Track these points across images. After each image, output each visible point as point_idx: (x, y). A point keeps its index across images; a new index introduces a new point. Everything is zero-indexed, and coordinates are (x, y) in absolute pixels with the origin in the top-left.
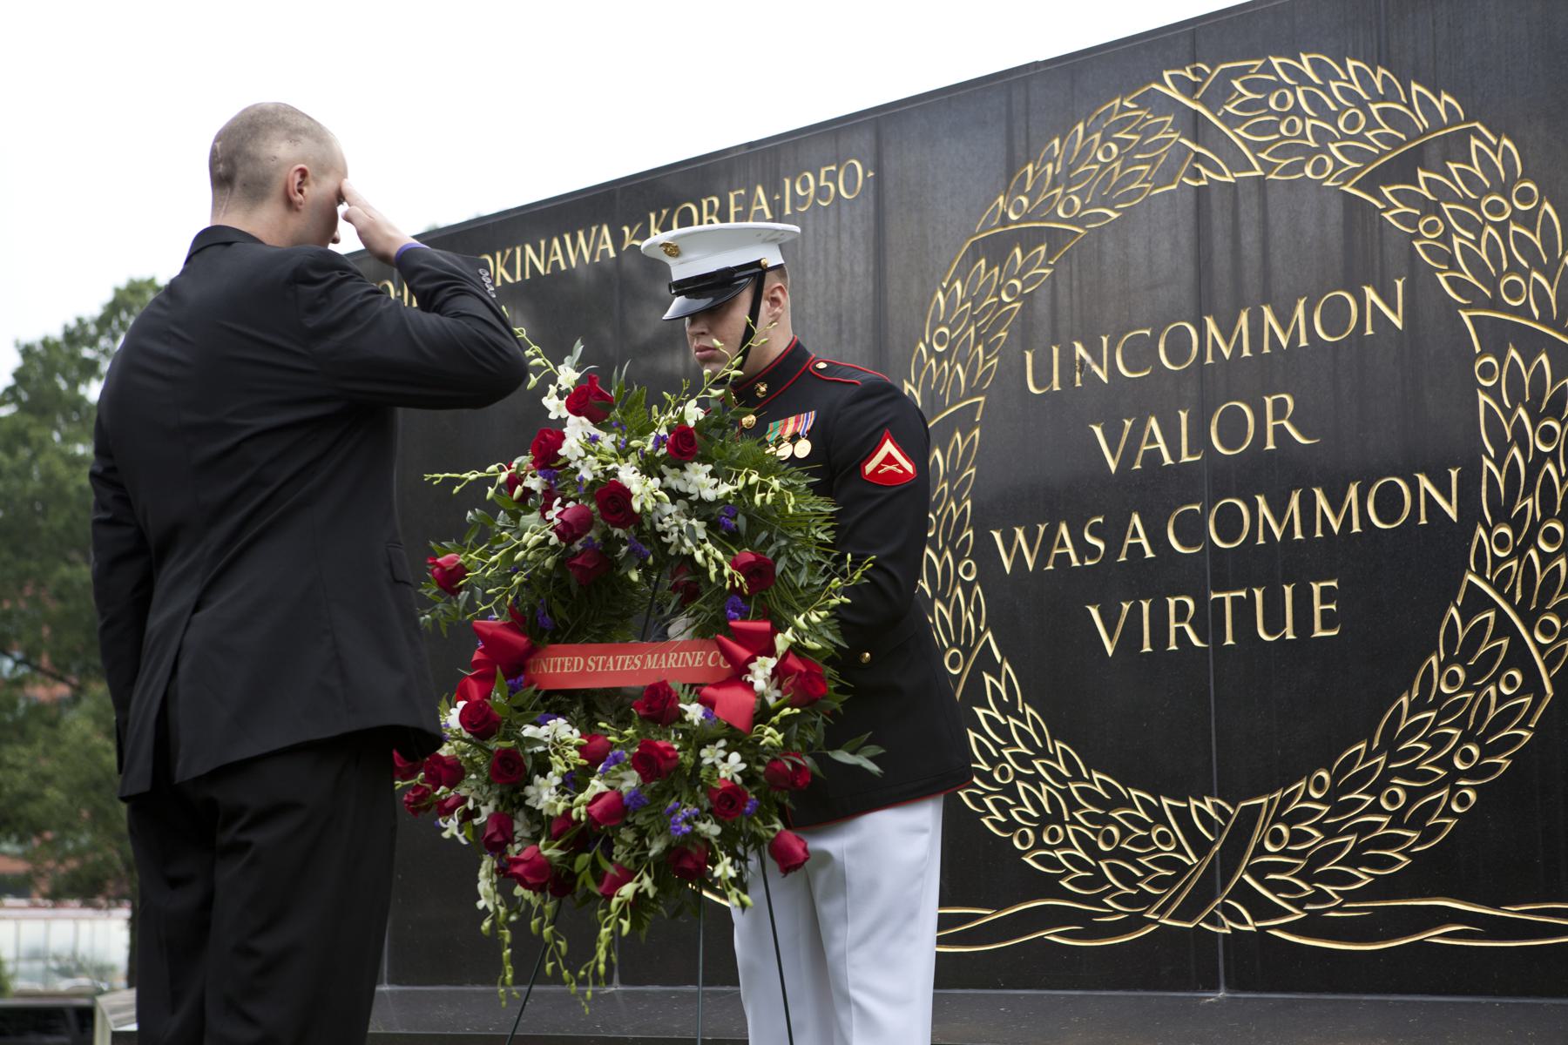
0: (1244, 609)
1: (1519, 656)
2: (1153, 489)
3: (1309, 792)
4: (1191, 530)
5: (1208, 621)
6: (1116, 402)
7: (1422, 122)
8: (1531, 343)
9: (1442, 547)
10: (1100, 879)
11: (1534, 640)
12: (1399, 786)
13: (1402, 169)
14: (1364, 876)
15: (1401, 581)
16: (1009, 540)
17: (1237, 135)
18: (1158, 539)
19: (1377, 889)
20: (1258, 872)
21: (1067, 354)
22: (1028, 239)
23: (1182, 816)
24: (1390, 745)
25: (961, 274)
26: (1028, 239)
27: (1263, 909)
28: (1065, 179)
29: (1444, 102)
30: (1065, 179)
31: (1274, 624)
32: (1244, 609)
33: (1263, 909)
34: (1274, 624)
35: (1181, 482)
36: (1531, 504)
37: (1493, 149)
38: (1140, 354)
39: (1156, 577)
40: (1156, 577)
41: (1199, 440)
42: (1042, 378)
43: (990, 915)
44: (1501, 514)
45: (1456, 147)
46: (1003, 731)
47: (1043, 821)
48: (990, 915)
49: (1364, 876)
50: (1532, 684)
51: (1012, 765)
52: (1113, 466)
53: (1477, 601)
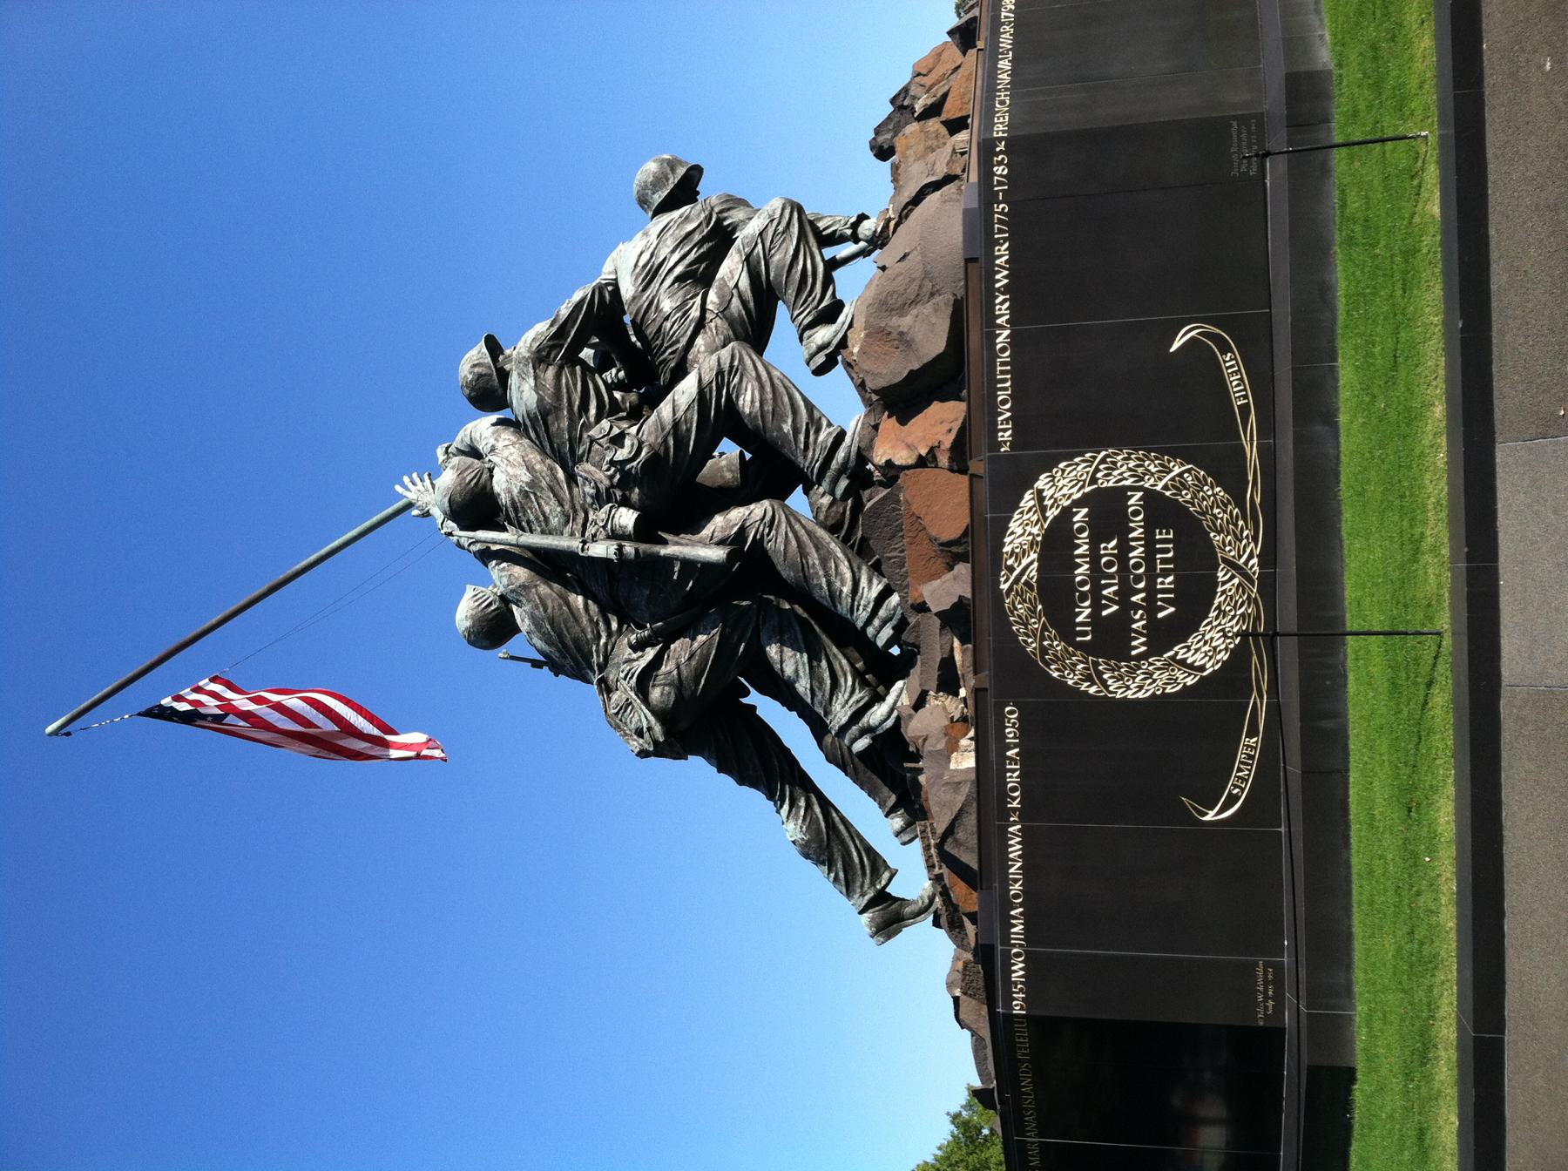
1: (1180, 475)
2: (1125, 592)
3: (1217, 539)
4: (1138, 579)
5: (1165, 573)
6: (1097, 607)
7: (1032, 503)
8: (1097, 470)
9: (1150, 497)
10: (1242, 615)
11: (1177, 470)
12: (1216, 511)
13: (1043, 509)
14: (1241, 523)
15: (1160, 509)
16: (1136, 648)
17: (1025, 562)
18: (1140, 591)
20: (1240, 557)
21: (1082, 624)
23: (1224, 583)
25: (1048, 665)
26: (1043, 638)
27: (1251, 556)
28: (1026, 625)
30: (1026, 625)
31: (1167, 550)
32: (1164, 561)
33: (1251, 556)
34: (1167, 550)
36: (1140, 470)
37: (1042, 482)
38: (1083, 597)
39: (1151, 591)
40: (1151, 591)
41: (1111, 577)
42: (1085, 634)
43: (1255, 657)
45: (1040, 492)
46: (1197, 650)
47: (1225, 636)
48: (1255, 657)
49: (1241, 523)
50: (1189, 471)
51: (1207, 648)
52: (1116, 607)
53: (1166, 487)
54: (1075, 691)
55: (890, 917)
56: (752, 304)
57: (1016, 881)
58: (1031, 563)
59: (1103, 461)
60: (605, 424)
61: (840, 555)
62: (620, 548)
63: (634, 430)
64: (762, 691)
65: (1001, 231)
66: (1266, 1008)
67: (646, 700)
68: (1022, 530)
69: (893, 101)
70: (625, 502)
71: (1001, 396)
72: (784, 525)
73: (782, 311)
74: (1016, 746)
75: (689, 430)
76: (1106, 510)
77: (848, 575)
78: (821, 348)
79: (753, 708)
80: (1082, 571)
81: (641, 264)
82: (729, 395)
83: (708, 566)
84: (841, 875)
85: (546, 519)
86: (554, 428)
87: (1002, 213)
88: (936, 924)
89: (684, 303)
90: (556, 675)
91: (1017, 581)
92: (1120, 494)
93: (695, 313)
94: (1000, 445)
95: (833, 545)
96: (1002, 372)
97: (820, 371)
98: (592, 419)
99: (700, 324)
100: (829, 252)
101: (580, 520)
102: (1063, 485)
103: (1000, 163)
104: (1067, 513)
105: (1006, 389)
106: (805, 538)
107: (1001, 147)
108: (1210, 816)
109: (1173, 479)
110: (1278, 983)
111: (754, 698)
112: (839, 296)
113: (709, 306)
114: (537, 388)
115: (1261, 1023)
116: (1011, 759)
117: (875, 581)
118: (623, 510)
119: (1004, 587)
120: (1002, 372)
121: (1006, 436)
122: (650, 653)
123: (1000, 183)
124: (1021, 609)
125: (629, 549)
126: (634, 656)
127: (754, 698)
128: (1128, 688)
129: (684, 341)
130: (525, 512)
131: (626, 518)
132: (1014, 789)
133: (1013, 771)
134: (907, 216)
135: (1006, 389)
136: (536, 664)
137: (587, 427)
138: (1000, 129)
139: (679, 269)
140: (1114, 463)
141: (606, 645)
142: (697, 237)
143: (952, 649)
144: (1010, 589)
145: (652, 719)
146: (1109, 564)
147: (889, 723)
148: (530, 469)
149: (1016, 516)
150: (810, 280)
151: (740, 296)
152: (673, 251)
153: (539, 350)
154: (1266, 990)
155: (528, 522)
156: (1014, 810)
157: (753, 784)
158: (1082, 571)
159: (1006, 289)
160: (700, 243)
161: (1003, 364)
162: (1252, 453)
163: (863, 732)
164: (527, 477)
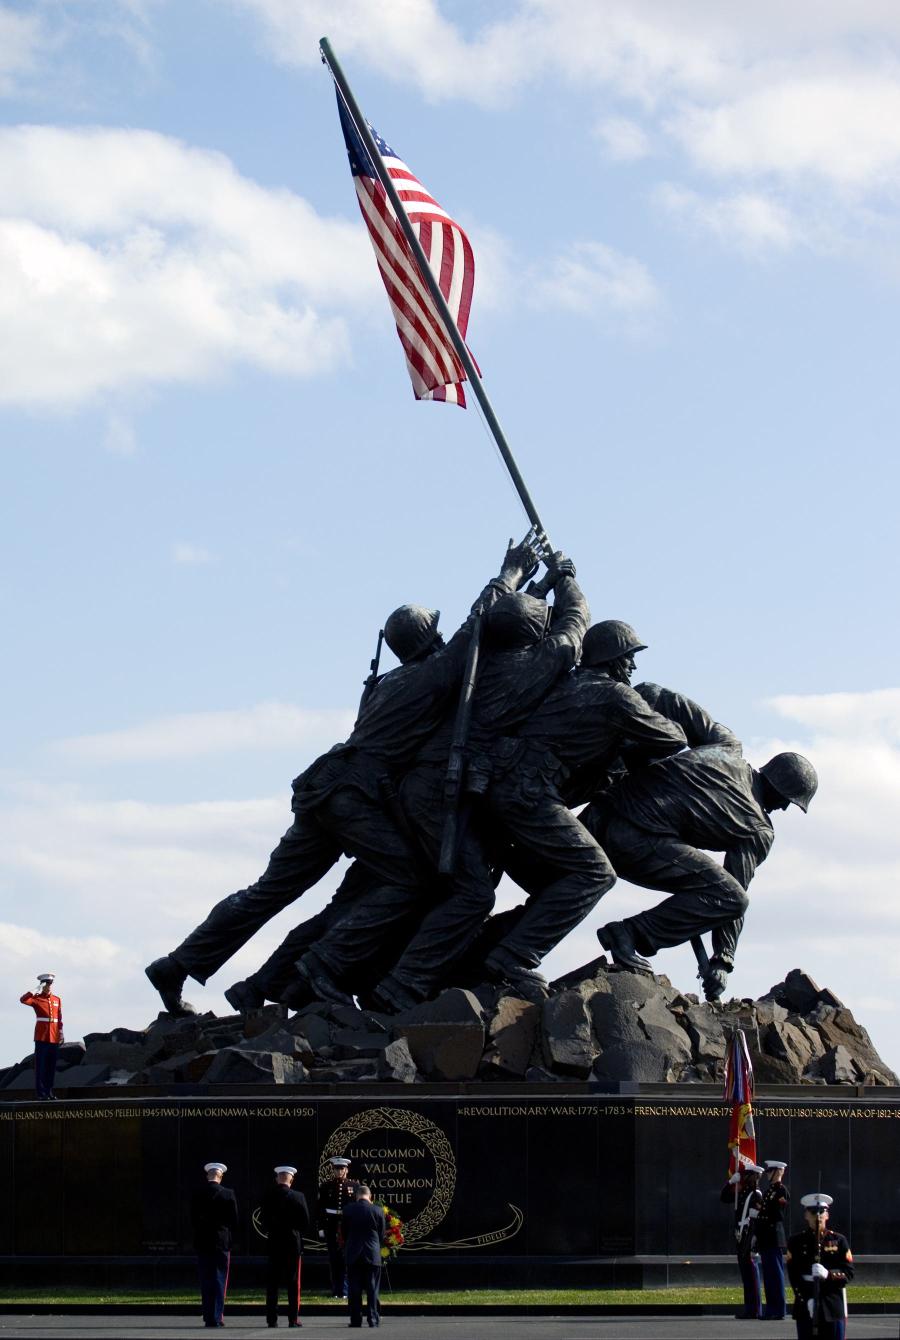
0: (394, 1198)
1: (441, 1208)
4: (384, 1183)
8: (445, 1162)
14: (414, 1239)
17: (395, 1121)
18: (377, 1184)
19: (416, 1241)
21: (360, 1153)
22: (352, 1131)
24: (419, 1220)
26: (352, 1131)
28: (360, 1121)
29: (432, 1123)
30: (360, 1121)
31: (400, 1199)
32: (394, 1198)
34: (400, 1199)
35: (382, 1176)
38: (374, 1153)
41: (386, 1169)
42: (354, 1154)
44: (439, 1187)
45: (434, 1131)
50: (443, 1212)
53: (434, 1199)
54: (322, 1148)
55: (166, 976)
57: (217, 1112)
58: (395, 1125)
59: (450, 1166)
61: (446, 958)
62: (455, 782)
63: (553, 791)
64: (350, 872)
66: (152, 1246)
68: (413, 1123)
69: (825, 991)
70: (492, 782)
71: (490, 1111)
74: (292, 1114)
76: (423, 1167)
77: (431, 965)
78: (616, 939)
79: (337, 860)
80: (389, 1153)
83: (437, 858)
84: (201, 942)
85: (486, 706)
87: (593, 1111)
88: (161, 1014)
90: (365, 683)
91: (385, 1116)
92: (431, 1175)
93: (656, 827)
94: (462, 1108)
95: (454, 952)
96: (503, 1110)
97: (601, 933)
98: (561, 754)
99: (646, 833)
100: (707, 939)
102: (439, 1143)
103: (620, 1110)
104: (421, 1145)
105: (493, 1112)
107: (629, 1111)
108: (255, 1219)
109: (439, 1203)
111: (344, 863)
112: (661, 951)
116: (284, 1111)
117: (423, 986)
119: (381, 1110)
120: (503, 1110)
121: (466, 1112)
123: (609, 1110)
124: (368, 1120)
125: (451, 790)
127: (344, 863)
128: (324, 1177)
131: (479, 786)
132: (267, 1112)
133: (278, 1112)
134: (681, 1024)
135: (493, 1112)
136: (375, 664)
138: (640, 1110)
140: (449, 1172)
143: (363, 1057)
144: (380, 1113)
146: (393, 1168)
147: (318, 992)
148: (528, 692)
149: (421, 1117)
154: (162, 1246)
156: (256, 1112)
158: (389, 1153)
161: (507, 1110)
162: (450, 1246)
163: (311, 971)
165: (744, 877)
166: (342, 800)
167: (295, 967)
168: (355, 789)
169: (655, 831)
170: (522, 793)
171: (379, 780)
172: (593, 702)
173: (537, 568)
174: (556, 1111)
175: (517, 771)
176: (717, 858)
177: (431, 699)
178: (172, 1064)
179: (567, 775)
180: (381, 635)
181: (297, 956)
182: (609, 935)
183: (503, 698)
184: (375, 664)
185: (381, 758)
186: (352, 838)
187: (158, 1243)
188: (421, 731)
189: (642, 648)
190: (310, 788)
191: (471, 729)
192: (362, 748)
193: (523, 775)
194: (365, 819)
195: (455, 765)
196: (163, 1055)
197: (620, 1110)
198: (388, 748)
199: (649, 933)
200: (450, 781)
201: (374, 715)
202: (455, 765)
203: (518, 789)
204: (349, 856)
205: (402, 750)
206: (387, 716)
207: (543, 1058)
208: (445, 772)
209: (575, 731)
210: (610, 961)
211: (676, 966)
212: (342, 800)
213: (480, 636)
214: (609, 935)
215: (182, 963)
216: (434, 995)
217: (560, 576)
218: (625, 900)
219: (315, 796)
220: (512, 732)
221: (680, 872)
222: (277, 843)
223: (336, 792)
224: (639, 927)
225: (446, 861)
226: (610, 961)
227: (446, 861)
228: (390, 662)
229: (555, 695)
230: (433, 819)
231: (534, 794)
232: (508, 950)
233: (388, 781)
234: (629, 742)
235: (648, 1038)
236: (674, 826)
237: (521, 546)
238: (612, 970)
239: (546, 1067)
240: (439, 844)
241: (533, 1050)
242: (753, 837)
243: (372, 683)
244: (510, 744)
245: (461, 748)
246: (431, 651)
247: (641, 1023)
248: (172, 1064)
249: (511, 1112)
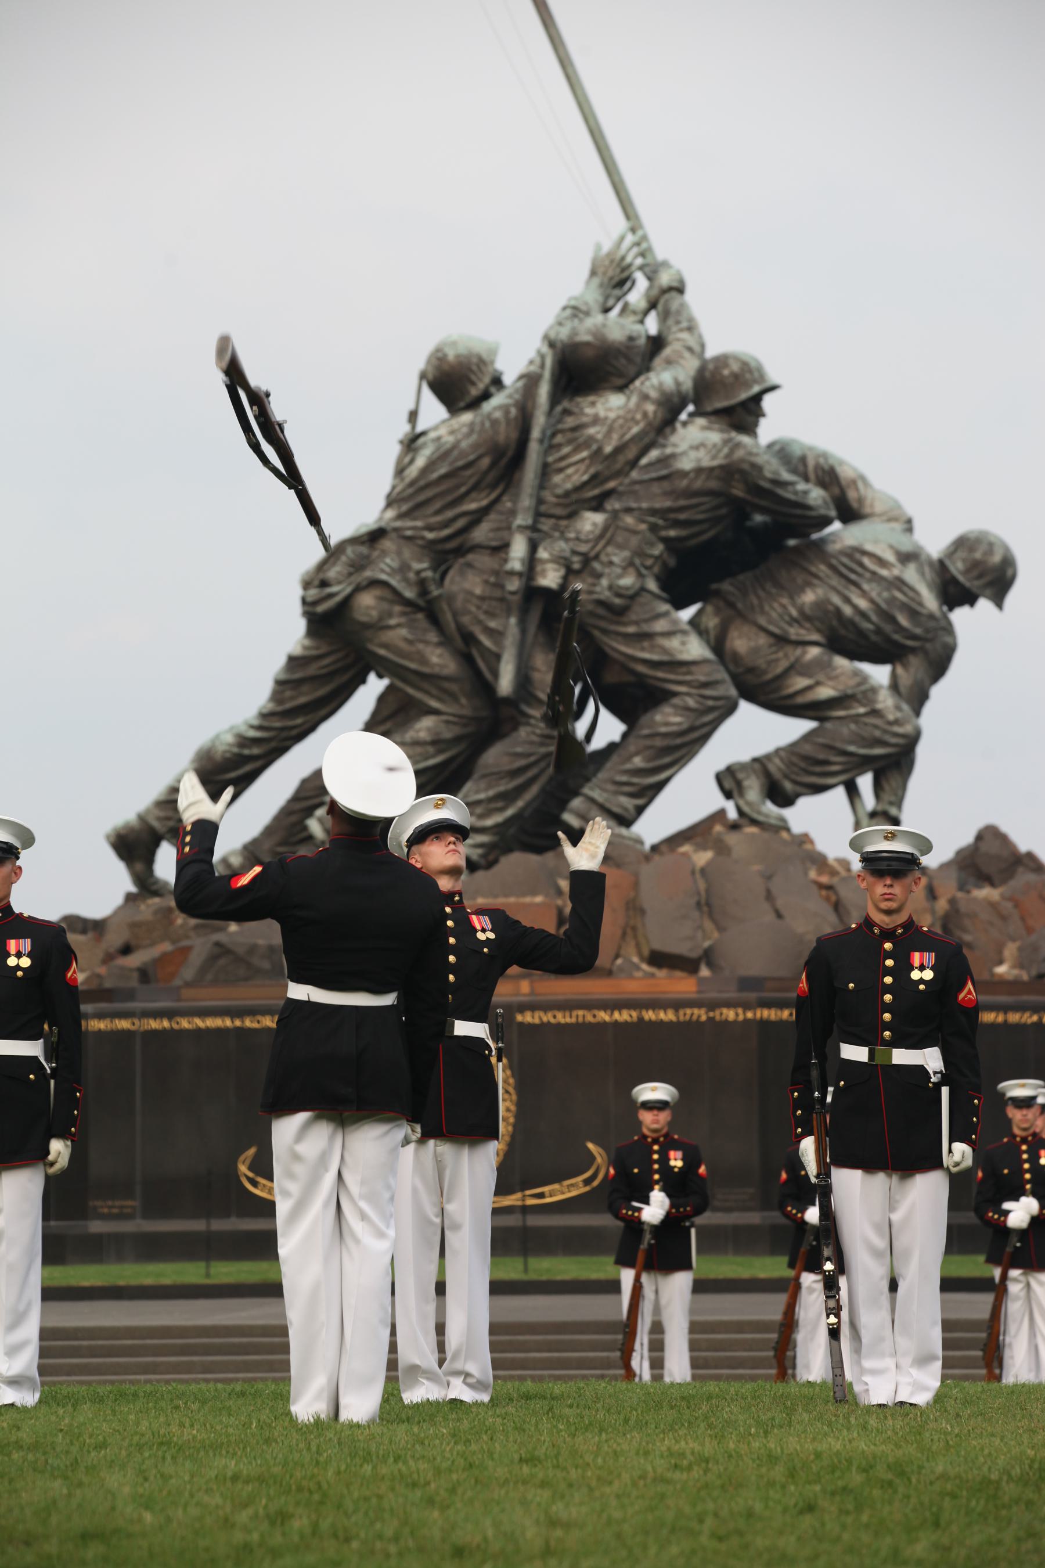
56: (800, 700)
60: (658, 549)
62: (520, 574)
63: (652, 585)
64: (382, 699)
65: (685, 1015)
66: (102, 1207)
67: (358, 589)
70: (570, 573)
72: (543, 750)
73: (802, 726)
75: (643, 649)
77: (489, 822)
78: (739, 784)
79: (363, 681)
81: (866, 561)
82: (675, 694)
83: (496, 674)
85: (561, 470)
86: (656, 488)
88: (129, 898)
89: (808, 618)
90: (401, 442)
93: (794, 632)
97: (719, 778)
98: (664, 533)
99: (782, 640)
100: (865, 782)
101: (559, 511)
103: (737, 1015)
106: (530, 774)
110: (121, 1216)
113: (799, 651)
114: (699, 471)
115: (91, 1204)
118: (562, 572)
122: (409, 594)
125: (514, 585)
126: (411, 576)
129: (762, 621)
130: (569, 442)
131: (550, 578)
134: (827, 899)
136: (413, 416)
137: (654, 528)
139: (847, 610)
141: (423, 538)
142: (888, 628)
145: (338, 599)
148: (618, 450)
150: (818, 769)
151: (809, 688)
152: (872, 601)
153: (742, 472)
155: (559, 446)
157: (277, 696)
159: (641, 1019)
160: (879, 631)
164: (608, 449)
165: (918, 699)
166: (367, 600)
167: (305, 828)
168: (385, 584)
169: (793, 637)
170: (610, 588)
171: (418, 573)
172: (707, 462)
173: (634, 283)
174: (649, 1015)
175: (604, 558)
176: (880, 674)
177: (486, 462)
178: (135, 960)
179: (672, 562)
180: (423, 376)
181: (309, 812)
182: (729, 781)
183: (582, 460)
184: (413, 416)
185: (420, 542)
186: (382, 652)
187: (110, 1203)
188: (473, 506)
189: (773, 388)
190: (324, 584)
191: (540, 501)
192: (396, 530)
193: (611, 563)
194: (399, 625)
195: (519, 548)
196: (126, 950)
197: (737, 1015)
198: (430, 528)
199: (786, 776)
200: (512, 573)
201: (412, 483)
202: (519, 548)
203: (605, 582)
204: (380, 676)
205: (446, 532)
206: (428, 486)
207: (638, 946)
208: (506, 561)
209: (682, 502)
210: (732, 814)
211: (825, 821)
212: (367, 600)
213: (553, 374)
214: (729, 781)
215: (156, 824)
216: (490, 865)
217: (667, 296)
218: (754, 732)
219: (331, 596)
220: (597, 505)
221: (825, 692)
222: (281, 661)
223: (358, 589)
224: (772, 768)
225: (505, 683)
226: (732, 814)
227: (505, 683)
228: (433, 412)
229: (654, 454)
230: (493, 624)
231: (627, 588)
232: (592, 800)
233: (429, 574)
234: (759, 518)
235: (779, 915)
236: (819, 631)
237: (609, 254)
238: (735, 827)
239: (642, 958)
240: (498, 657)
241: (624, 934)
242: (928, 646)
243: (411, 443)
244: (591, 521)
245: (526, 528)
246: (486, 396)
247: (769, 896)
248: (135, 960)
249: (589, 1018)
